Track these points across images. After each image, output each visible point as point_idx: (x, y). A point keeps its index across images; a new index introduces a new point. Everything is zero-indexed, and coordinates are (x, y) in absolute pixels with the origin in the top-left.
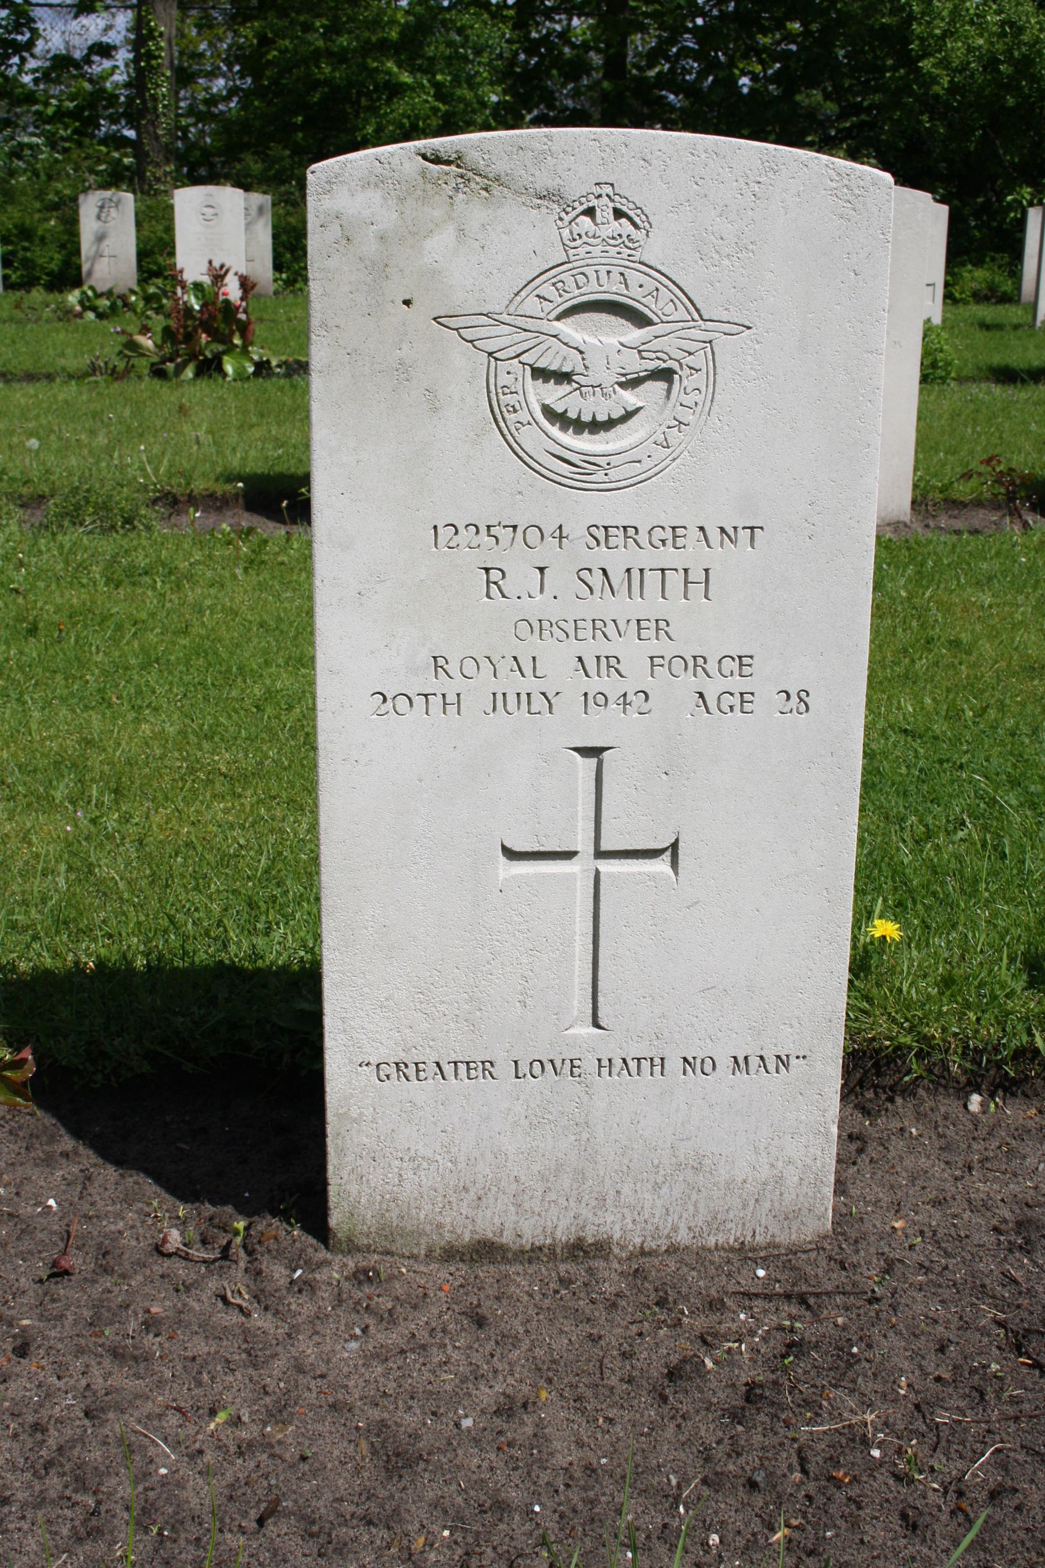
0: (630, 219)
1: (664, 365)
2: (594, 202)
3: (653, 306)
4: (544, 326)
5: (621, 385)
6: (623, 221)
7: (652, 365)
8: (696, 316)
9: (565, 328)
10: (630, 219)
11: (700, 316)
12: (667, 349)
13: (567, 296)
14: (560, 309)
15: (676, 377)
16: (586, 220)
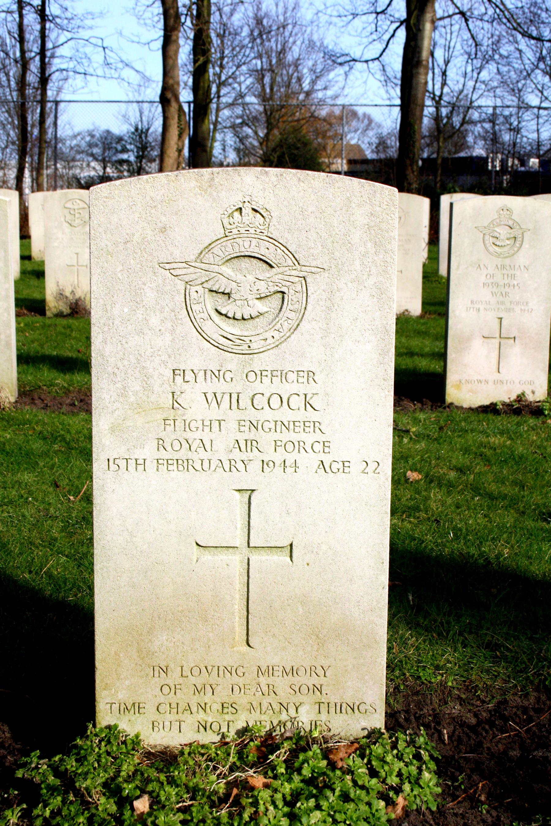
0: (260, 214)
1: (279, 290)
2: (241, 206)
3: (274, 260)
4: (216, 269)
5: (257, 299)
6: (258, 215)
7: (273, 289)
8: (296, 263)
9: (227, 270)
10: (260, 214)
11: (299, 264)
12: (281, 281)
13: (227, 253)
14: (225, 260)
15: (286, 296)
16: (237, 214)
